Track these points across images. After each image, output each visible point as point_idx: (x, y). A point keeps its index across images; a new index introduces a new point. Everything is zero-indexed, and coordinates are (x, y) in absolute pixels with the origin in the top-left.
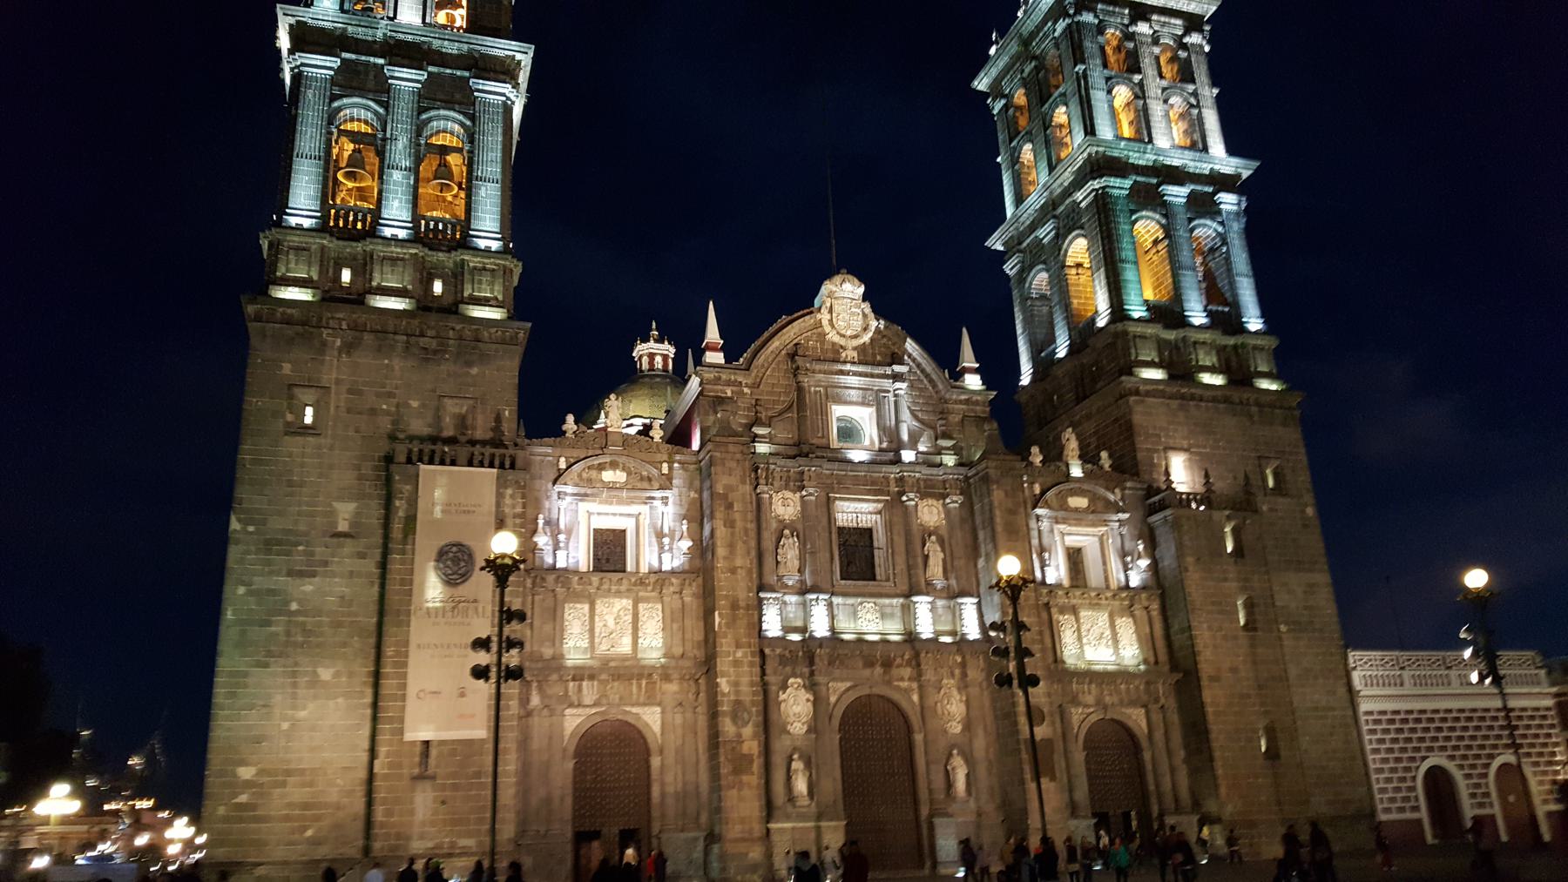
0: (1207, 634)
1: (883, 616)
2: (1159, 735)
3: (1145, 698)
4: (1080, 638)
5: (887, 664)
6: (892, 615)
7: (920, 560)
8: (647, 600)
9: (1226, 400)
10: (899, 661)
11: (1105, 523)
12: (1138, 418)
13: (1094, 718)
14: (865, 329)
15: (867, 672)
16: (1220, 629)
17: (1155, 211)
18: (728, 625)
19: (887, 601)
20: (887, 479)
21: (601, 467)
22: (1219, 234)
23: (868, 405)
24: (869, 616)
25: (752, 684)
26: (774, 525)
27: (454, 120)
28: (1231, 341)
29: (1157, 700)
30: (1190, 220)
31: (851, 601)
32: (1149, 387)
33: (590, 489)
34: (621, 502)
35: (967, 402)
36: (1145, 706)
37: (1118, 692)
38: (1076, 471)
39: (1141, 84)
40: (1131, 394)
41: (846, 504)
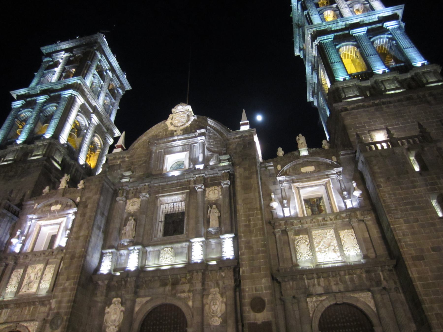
0: (404, 226)
1: (176, 254)
2: (383, 312)
3: (368, 283)
4: (312, 249)
5: (175, 283)
6: (181, 254)
7: (201, 219)
8: (52, 263)
9: (408, 99)
10: (183, 280)
11: (327, 176)
12: (348, 121)
13: (327, 304)
14: (188, 121)
15: (161, 290)
16: (416, 220)
17: (349, 41)
18: (66, 268)
19: (179, 245)
20: (189, 182)
21: (51, 205)
22: (389, 39)
23: (186, 151)
24: (167, 256)
25: (69, 302)
26: (125, 216)
27: (54, 106)
28: (409, 75)
29: (379, 283)
30: (370, 39)
31: (157, 248)
32: (352, 106)
33: (44, 214)
34: (55, 218)
35: (240, 137)
36: (369, 290)
37: (343, 281)
38: (304, 152)
39: (337, 7)
40: (342, 111)
41: (165, 198)
